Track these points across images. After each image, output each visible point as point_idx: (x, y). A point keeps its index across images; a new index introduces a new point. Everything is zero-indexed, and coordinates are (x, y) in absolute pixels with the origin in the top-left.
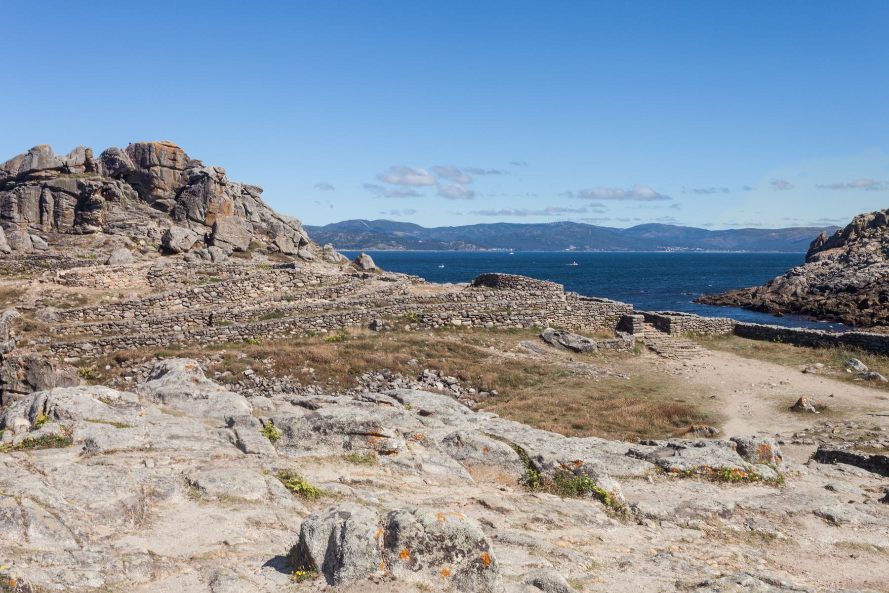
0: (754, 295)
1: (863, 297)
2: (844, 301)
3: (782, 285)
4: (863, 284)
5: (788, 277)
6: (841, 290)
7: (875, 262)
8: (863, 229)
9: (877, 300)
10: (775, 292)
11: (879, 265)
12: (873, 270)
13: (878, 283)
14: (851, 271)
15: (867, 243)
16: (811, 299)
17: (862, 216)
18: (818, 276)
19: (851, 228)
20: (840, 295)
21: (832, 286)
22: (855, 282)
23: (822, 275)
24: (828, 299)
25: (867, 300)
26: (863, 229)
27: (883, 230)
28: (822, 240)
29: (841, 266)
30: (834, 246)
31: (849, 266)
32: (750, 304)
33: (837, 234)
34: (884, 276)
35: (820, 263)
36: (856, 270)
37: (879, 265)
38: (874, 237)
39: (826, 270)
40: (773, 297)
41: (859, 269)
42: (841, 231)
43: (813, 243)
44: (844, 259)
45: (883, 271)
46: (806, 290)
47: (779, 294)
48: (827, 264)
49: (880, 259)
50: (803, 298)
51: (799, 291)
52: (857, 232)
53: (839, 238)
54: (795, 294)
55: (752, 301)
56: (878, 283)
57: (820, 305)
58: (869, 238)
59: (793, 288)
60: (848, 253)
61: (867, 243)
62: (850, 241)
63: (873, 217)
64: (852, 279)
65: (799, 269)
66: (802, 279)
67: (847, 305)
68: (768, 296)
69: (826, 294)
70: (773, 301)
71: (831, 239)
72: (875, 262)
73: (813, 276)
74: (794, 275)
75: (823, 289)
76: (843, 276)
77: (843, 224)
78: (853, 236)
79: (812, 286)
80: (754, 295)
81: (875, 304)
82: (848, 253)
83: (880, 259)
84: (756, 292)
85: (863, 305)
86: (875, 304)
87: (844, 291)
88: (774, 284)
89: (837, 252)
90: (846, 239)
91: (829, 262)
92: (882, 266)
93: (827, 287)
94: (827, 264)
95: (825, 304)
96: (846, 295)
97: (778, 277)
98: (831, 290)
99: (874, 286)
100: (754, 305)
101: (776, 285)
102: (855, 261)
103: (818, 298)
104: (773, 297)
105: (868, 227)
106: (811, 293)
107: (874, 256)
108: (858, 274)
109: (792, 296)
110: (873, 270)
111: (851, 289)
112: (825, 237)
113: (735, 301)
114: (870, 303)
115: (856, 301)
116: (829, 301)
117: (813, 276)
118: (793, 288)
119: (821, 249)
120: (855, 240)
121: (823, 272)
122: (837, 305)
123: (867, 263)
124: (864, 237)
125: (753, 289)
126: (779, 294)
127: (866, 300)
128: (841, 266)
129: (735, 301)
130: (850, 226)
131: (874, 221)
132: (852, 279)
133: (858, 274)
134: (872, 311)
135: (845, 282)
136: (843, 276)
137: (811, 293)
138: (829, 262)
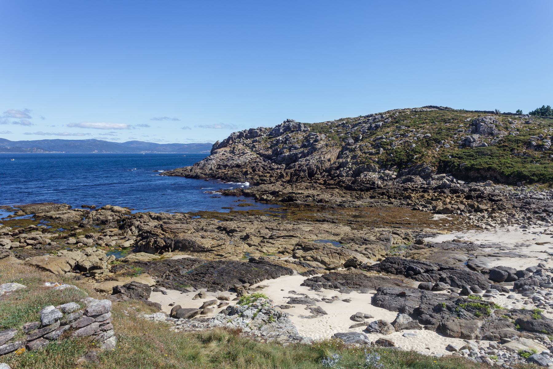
1: (244, 170)
3: (204, 165)
4: (243, 163)
6: (233, 167)
7: (247, 153)
9: (251, 170)
11: (249, 154)
13: (250, 163)
16: (220, 171)
18: (221, 160)
20: (234, 169)
21: (229, 165)
22: (240, 162)
23: (223, 159)
24: (228, 171)
25: (247, 171)
29: (231, 155)
31: (235, 155)
32: (190, 175)
34: (252, 159)
36: (239, 157)
37: (249, 154)
39: (224, 157)
40: (201, 171)
41: (240, 156)
42: (226, 140)
44: (232, 152)
45: (251, 157)
46: (216, 167)
47: (203, 169)
51: (213, 168)
54: (211, 169)
55: (191, 174)
56: (250, 163)
59: (210, 166)
64: (238, 161)
66: (214, 162)
68: (198, 171)
69: (227, 169)
70: (201, 173)
72: (247, 153)
73: (219, 160)
75: (225, 166)
76: (234, 160)
77: (226, 137)
81: (251, 173)
84: (192, 169)
86: (251, 173)
87: (235, 167)
90: (228, 143)
92: (251, 155)
96: (236, 169)
98: (229, 167)
99: (248, 164)
100: (192, 175)
103: (224, 171)
104: (201, 171)
109: (210, 170)
110: (247, 156)
111: (238, 166)
113: (181, 174)
114: (249, 172)
115: (242, 172)
117: (219, 160)
118: (210, 166)
126: (203, 169)
127: (247, 171)
128: (231, 155)
129: (181, 174)
132: (238, 161)
134: (251, 176)
135: (235, 162)
136: (234, 160)
137: (220, 168)
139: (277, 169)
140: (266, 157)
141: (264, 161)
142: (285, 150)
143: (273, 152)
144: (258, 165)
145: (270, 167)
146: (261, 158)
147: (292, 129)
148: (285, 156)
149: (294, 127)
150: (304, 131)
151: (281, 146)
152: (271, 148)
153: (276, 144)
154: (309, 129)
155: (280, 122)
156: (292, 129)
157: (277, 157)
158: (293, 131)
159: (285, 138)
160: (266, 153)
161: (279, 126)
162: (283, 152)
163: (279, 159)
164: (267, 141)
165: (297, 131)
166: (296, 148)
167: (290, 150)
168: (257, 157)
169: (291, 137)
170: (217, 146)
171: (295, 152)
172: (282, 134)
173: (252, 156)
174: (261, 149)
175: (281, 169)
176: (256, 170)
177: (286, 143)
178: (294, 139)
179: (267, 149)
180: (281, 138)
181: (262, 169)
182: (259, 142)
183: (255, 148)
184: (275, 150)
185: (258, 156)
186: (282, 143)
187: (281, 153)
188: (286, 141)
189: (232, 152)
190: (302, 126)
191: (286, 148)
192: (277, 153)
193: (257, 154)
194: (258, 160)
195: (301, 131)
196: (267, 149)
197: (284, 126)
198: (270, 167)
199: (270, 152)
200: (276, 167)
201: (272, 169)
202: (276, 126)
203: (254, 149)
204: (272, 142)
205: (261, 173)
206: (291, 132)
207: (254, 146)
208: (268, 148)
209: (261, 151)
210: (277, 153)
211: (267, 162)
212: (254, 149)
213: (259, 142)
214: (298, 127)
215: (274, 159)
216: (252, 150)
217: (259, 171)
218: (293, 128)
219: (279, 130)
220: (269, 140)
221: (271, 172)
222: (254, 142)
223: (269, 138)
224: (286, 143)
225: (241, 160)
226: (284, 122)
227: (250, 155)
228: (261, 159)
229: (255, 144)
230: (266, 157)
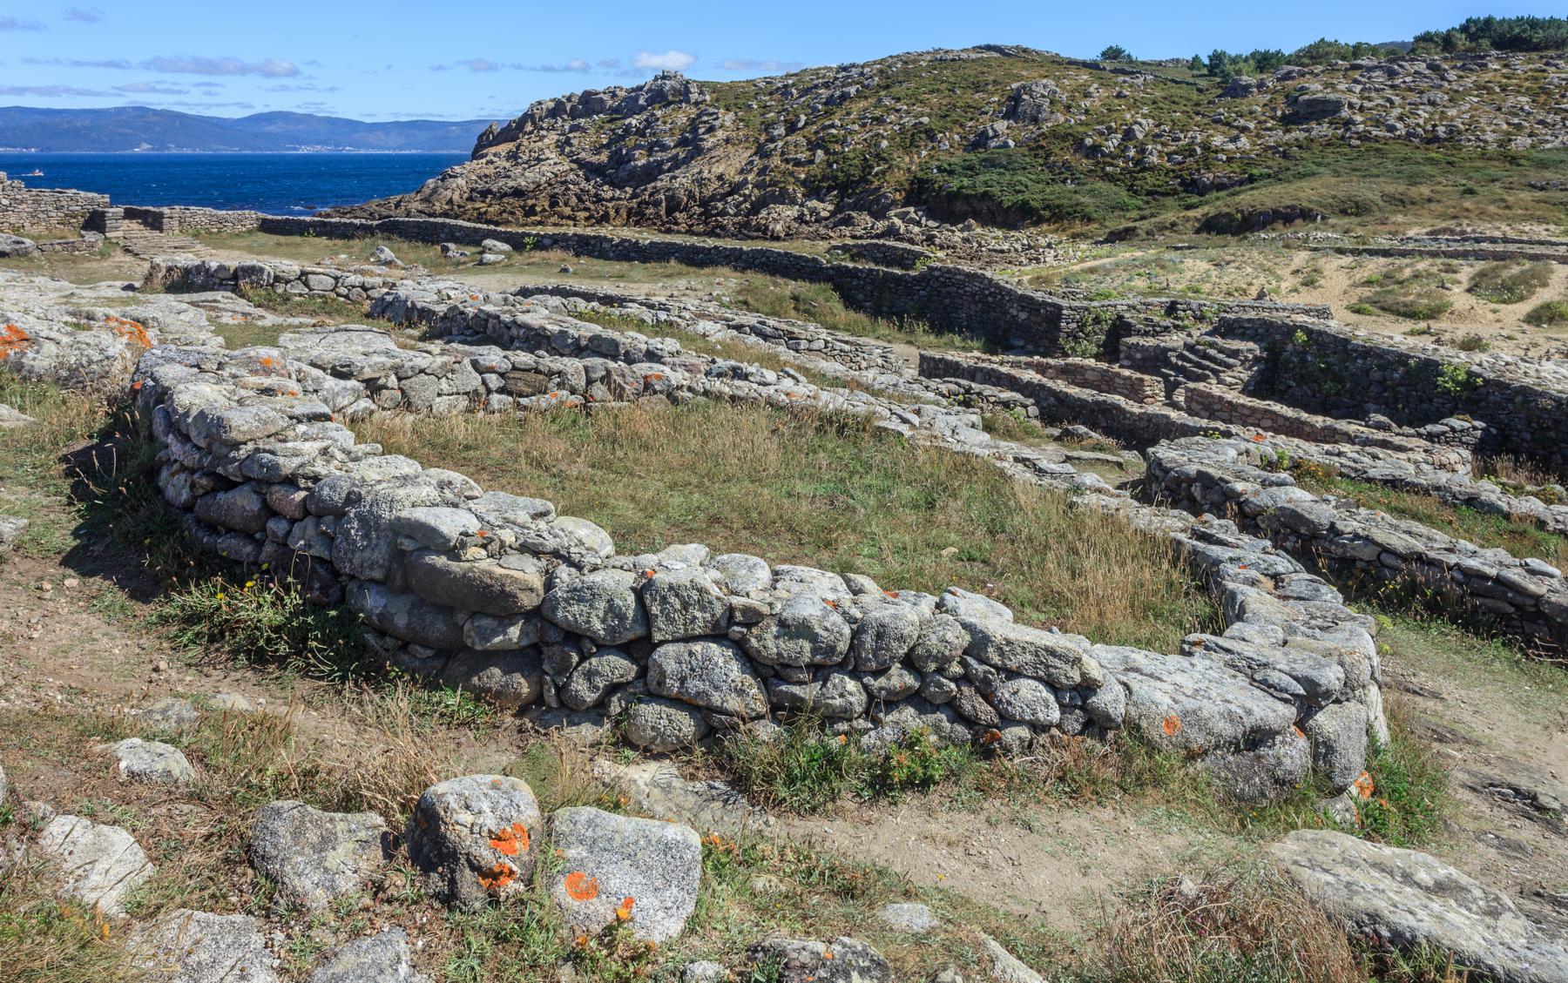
0: (397, 205)
1: (530, 202)
2: (509, 208)
3: (435, 191)
4: (532, 186)
5: (443, 180)
6: (506, 195)
8: (541, 119)
9: (546, 204)
10: (426, 200)
12: (544, 168)
13: (550, 185)
14: (519, 170)
15: (544, 136)
17: (540, 103)
18: (480, 178)
19: (527, 117)
20: (505, 200)
22: (523, 183)
23: (486, 176)
24: (490, 206)
26: (541, 119)
27: (564, 120)
28: (491, 132)
29: (507, 165)
30: (506, 141)
33: (509, 125)
34: (556, 176)
35: (484, 160)
36: (525, 169)
37: (552, 162)
38: (554, 129)
39: (490, 170)
43: (481, 137)
44: (513, 156)
45: (555, 170)
46: (466, 196)
48: (492, 162)
49: (553, 156)
50: (459, 206)
51: (456, 197)
52: (534, 123)
53: (512, 132)
54: (450, 202)
56: (550, 185)
57: (480, 214)
58: (548, 130)
60: (518, 148)
61: (544, 136)
62: (525, 133)
63: (552, 105)
65: (457, 169)
66: (461, 182)
67: (512, 213)
71: (503, 130)
73: (474, 178)
74: (451, 176)
75: (484, 194)
76: (509, 177)
78: (529, 127)
79: (472, 190)
80: (397, 205)
81: (544, 210)
82: (518, 148)
83: (553, 156)
85: (531, 211)
86: (544, 210)
88: (425, 189)
89: (504, 148)
91: (495, 159)
93: (489, 191)
94: (492, 162)
95: (486, 212)
97: (430, 181)
101: (427, 191)
102: (525, 158)
103: (478, 205)
105: (546, 117)
106: (470, 199)
107: (546, 151)
108: (527, 174)
110: (544, 168)
111: (518, 193)
112: (497, 129)
114: (538, 209)
115: (523, 207)
116: (491, 209)
117: (474, 178)
118: (449, 193)
119: (491, 145)
120: (532, 132)
121: (487, 172)
122: (501, 214)
123: (538, 160)
124: (542, 129)
125: (398, 198)
127: (534, 205)
128: (507, 165)
130: (525, 114)
131: (554, 109)
133: (527, 174)
135: (511, 183)
136: (509, 177)
137: (470, 199)
138: (495, 159)
139: (612, 199)
140: (591, 170)
141: (588, 180)
142: (637, 153)
143: (610, 158)
144: (568, 189)
145: (596, 195)
146: (581, 173)
147: (670, 98)
148: (636, 166)
149: (676, 92)
150: (697, 104)
151: (631, 141)
152: (607, 146)
153: (622, 138)
154: (708, 98)
155: (647, 79)
156: (670, 98)
157: (617, 169)
158: (670, 103)
159: (646, 120)
160: (594, 159)
161: (640, 88)
162: (631, 158)
163: (622, 174)
164: (601, 128)
165: (680, 102)
166: (664, 148)
167: (650, 152)
168: (572, 170)
169: (658, 119)
170: (488, 139)
171: (659, 156)
172: (642, 109)
173: (559, 167)
174: (583, 149)
175: (620, 199)
176: (558, 204)
177: (643, 135)
178: (665, 123)
179: (598, 150)
180: (634, 122)
181: (574, 200)
182: (584, 130)
183: (571, 145)
184: (616, 152)
185: (574, 166)
186: (636, 134)
187: (630, 161)
188: (646, 128)
189: (513, 156)
190: (694, 89)
191: (641, 147)
192: (618, 160)
193: (572, 161)
194: (571, 176)
195: (688, 102)
196: (598, 150)
197: (650, 90)
198: (596, 195)
199: (604, 157)
200: (610, 194)
201: (599, 200)
202: (633, 90)
203: (567, 149)
204: (613, 130)
205: (567, 211)
206: (665, 106)
207: (568, 142)
208: (603, 146)
209: (583, 155)
210: (618, 160)
211: (592, 182)
212: (567, 149)
213: (584, 130)
214: (683, 93)
215: (610, 175)
216: (562, 153)
217: (566, 205)
218: (673, 95)
219: (636, 99)
220: (608, 126)
221: (592, 207)
222: (573, 129)
223: (611, 121)
224: (643, 135)
225: (524, 178)
226: (656, 79)
227: (554, 164)
228: (578, 176)
229: (571, 135)
230: (591, 170)
